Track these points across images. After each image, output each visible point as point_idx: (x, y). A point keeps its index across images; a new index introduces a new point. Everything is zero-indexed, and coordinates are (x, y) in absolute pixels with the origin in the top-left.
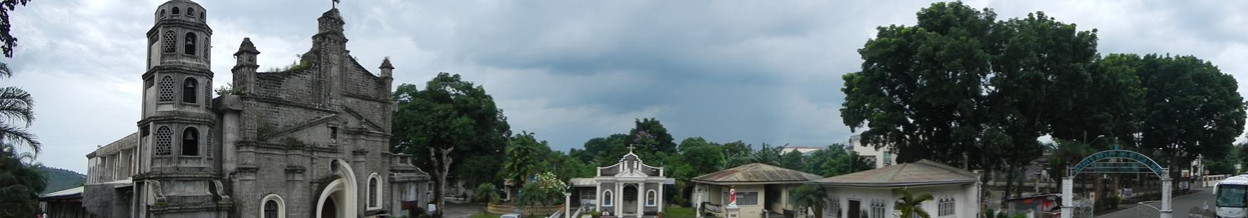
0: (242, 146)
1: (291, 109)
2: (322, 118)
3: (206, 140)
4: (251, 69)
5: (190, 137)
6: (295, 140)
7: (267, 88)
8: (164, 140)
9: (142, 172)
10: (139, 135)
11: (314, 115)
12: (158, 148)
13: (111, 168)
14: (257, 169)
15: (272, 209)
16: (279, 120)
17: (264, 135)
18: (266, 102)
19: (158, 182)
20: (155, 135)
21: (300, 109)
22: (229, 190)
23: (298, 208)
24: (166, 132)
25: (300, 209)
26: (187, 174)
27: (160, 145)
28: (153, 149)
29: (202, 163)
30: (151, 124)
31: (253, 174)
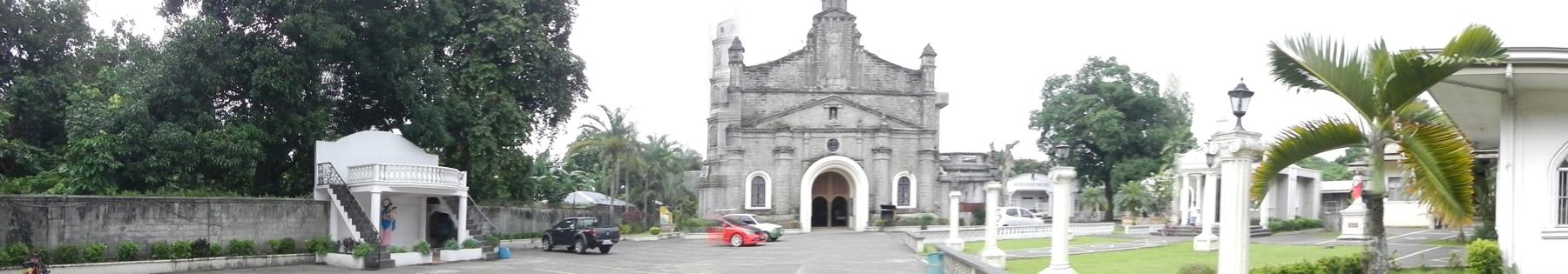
1: (781, 96)
11: (808, 98)
23: (783, 182)
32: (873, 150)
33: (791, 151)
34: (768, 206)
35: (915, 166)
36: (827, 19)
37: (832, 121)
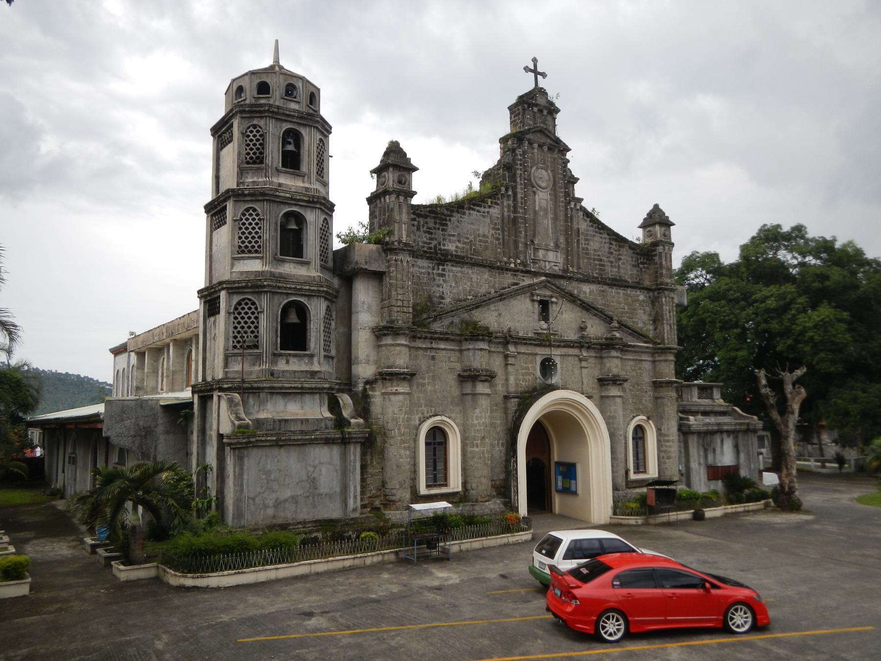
0: (385, 335)
1: (466, 269)
2: (522, 284)
3: (322, 325)
4: (402, 198)
5: (293, 318)
6: (475, 325)
7: (431, 233)
8: (246, 323)
9: (209, 379)
10: (202, 314)
11: (508, 279)
12: (235, 337)
13: (155, 371)
14: (413, 375)
15: (438, 440)
16: (446, 289)
17: (425, 316)
18: (428, 258)
19: (237, 395)
20: (229, 313)
21: (482, 269)
22: (363, 408)
23: (483, 438)
24: (250, 308)
25: (487, 440)
26: (289, 382)
27: (239, 332)
28: (227, 339)
29: (316, 363)
30: (223, 294)
31: (406, 384)
32: (600, 380)
33: (490, 377)
34: (455, 483)
35: (650, 405)
36: (531, 143)
37: (544, 325)
